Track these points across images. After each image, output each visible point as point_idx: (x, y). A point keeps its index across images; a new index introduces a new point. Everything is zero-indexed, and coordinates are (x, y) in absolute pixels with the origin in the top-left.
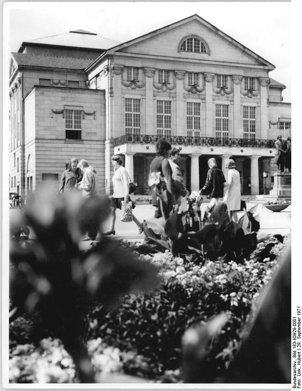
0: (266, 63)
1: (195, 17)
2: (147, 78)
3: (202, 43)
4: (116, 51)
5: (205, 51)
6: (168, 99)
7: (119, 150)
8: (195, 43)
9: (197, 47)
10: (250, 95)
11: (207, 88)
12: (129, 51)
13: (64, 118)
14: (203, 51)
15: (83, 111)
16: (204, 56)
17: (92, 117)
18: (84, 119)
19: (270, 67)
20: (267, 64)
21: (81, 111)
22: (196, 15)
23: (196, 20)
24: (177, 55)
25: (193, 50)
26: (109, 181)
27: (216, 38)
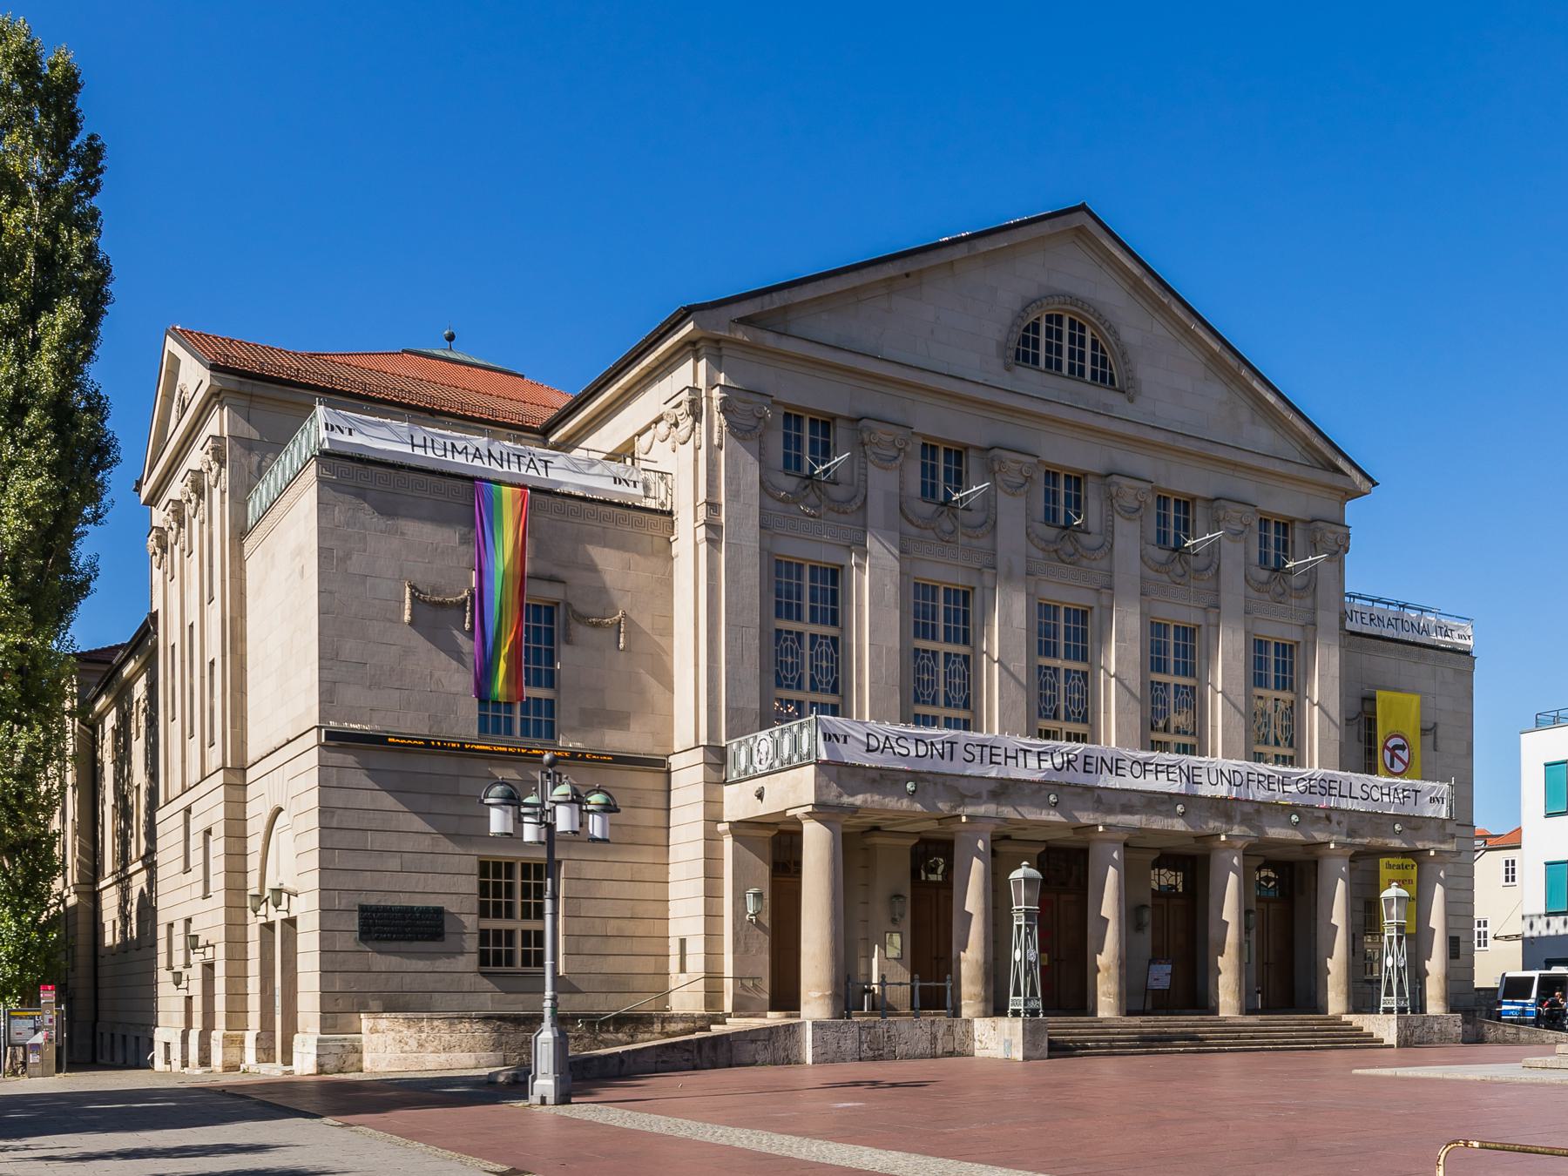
3: (1095, 343)
6: (959, 579)
7: (760, 796)
24: (1006, 380)
25: (1065, 370)
26: (696, 948)
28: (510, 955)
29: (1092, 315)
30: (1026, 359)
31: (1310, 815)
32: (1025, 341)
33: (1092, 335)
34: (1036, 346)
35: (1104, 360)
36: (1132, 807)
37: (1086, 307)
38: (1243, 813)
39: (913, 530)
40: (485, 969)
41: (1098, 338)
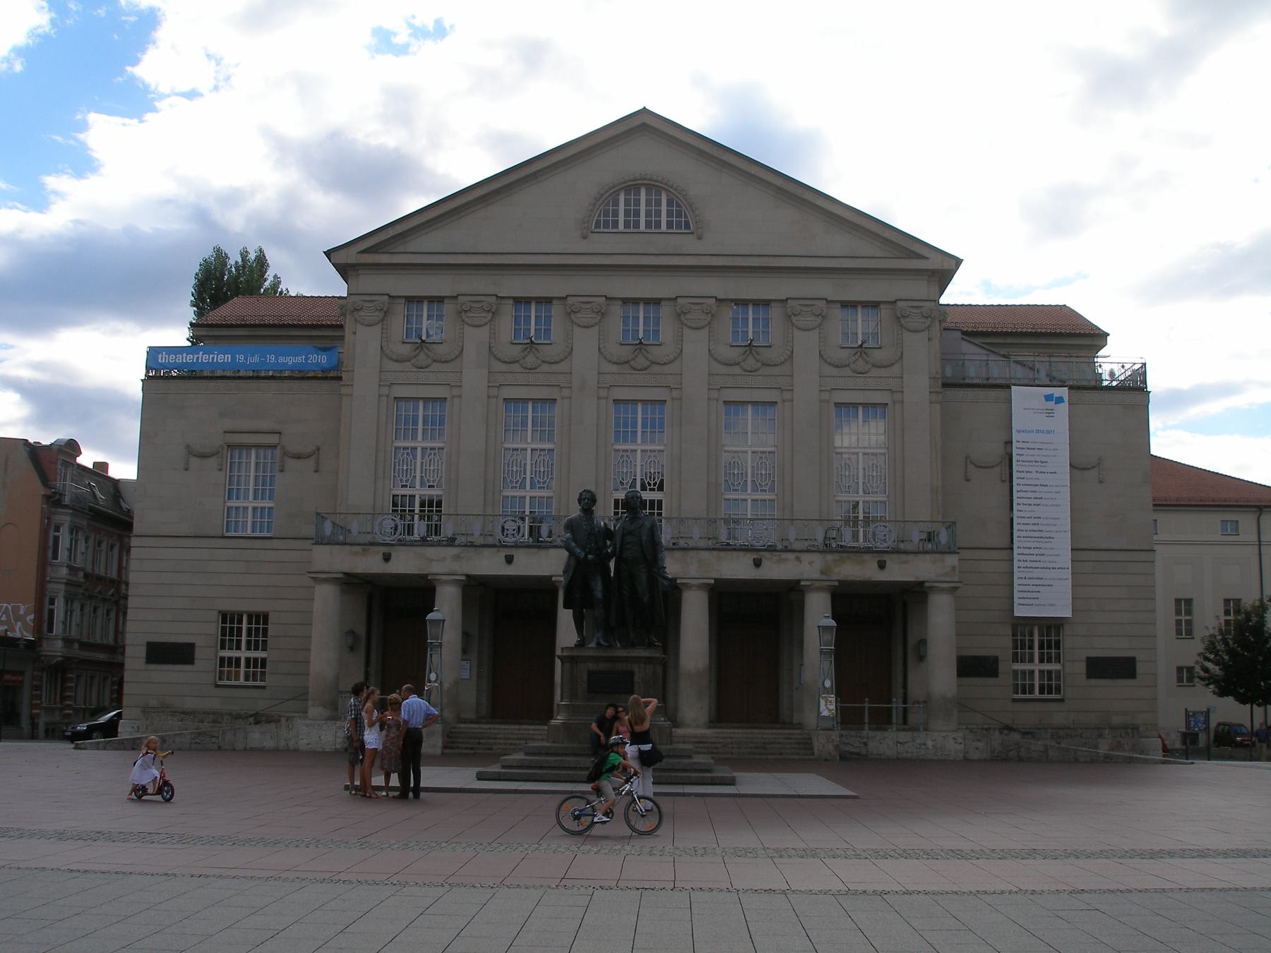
0: (917, 248)
1: (637, 122)
2: (468, 330)
3: (670, 203)
5: (687, 226)
8: (648, 203)
9: (653, 214)
10: (860, 365)
13: (220, 470)
15: (283, 448)
16: (687, 243)
17: (311, 463)
18: (282, 471)
20: (924, 252)
21: (275, 447)
22: (644, 111)
23: (644, 127)
24: (583, 246)
29: (661, 183)
30: (606, 225)
32: (606, 214)
33: (667, 196)
34: (616, 214)
35: (679, 215)
39: (503, 367)
41: (674, 197)
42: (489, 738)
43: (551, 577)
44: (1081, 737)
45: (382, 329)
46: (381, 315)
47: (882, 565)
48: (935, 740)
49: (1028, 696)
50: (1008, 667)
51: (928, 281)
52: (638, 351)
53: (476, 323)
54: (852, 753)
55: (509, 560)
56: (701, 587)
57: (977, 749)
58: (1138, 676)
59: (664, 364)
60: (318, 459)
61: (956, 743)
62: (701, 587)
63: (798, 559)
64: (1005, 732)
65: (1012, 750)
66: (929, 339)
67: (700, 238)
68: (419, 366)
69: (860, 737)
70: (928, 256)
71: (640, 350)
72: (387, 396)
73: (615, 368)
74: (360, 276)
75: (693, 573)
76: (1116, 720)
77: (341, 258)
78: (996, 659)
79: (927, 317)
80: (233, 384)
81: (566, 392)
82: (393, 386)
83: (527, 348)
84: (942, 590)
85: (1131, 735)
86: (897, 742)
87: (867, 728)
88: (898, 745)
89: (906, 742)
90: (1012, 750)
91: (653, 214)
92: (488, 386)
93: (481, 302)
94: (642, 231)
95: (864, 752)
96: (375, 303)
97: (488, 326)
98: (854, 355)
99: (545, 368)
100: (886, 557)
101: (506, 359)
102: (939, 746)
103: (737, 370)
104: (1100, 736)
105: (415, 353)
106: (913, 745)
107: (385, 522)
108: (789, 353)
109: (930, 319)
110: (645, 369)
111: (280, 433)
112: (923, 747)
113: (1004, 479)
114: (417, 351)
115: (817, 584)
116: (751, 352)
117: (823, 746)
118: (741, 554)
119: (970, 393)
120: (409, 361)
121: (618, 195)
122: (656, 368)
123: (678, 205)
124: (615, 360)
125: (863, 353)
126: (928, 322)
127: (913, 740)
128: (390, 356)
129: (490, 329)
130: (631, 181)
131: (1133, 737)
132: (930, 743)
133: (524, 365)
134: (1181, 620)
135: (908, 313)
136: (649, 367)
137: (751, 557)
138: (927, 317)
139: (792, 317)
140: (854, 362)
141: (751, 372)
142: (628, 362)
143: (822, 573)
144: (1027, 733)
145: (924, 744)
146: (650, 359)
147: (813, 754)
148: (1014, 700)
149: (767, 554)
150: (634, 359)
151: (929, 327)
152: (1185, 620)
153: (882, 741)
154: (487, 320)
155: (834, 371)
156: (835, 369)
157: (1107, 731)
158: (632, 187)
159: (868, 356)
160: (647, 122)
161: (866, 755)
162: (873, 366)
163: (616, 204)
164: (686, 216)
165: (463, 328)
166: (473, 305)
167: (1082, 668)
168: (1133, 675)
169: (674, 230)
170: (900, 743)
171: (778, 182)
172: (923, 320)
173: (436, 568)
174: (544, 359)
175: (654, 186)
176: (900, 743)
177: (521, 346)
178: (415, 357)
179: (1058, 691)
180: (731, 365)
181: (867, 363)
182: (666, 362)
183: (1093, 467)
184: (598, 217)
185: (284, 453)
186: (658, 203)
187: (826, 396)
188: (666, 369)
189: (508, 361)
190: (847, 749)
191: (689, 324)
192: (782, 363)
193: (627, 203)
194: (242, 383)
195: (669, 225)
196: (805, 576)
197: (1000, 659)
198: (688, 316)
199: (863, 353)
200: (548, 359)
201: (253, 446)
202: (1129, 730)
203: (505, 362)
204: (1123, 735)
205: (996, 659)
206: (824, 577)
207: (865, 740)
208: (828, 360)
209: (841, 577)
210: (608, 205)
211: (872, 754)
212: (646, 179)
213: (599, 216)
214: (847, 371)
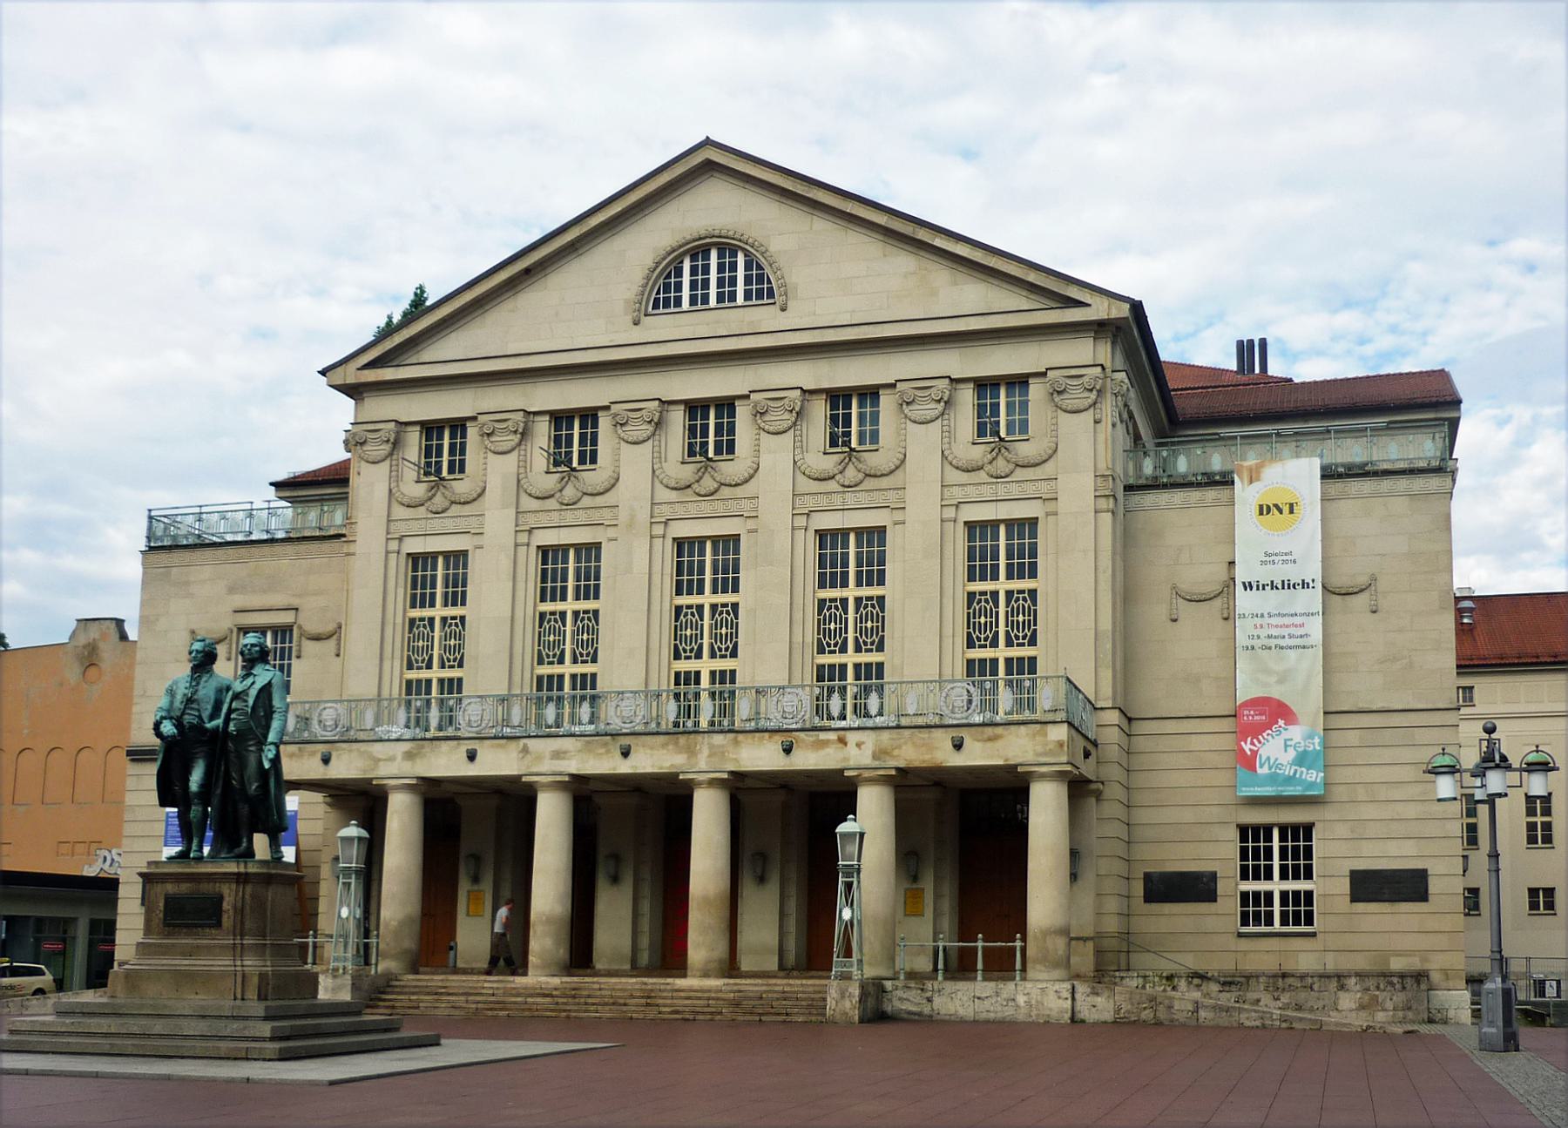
0: (1074, 292)
3: (748, 266)
4: (371, 365)
5: (771, 294)
8: (721, 268)
9: (726, 283)
11: (765, 461)
12: (427, 355)
14: (762, 289)
15: (300, 627)
17: (332, 642)
18: (298, 657)
19: (1099, 310)
23: (709, 167)
24: (636, 335)
27: (822, 226)
28: (1270, 915)
29: (733, 239)
30: (667, 304)
31: (811, 739)
33: (746, 256)
36: (565, 752)
37: (724, 233)
38: (711, 746)
40: (1245, 930)
42: (589, 996)
43: (520, 776)
44: (1311, 988)
45: (391, 466)
46: (387, 447)
47: (958, 746)
48: (1028, 994)
49: (1263, 929)
50: (1232, 886)
51: (1095, 338)
52: (702, 470)
53: (500, 449)
54: (910, 1013)
55: (472, 756)
56: (713, 783)
57: (1094, 1006)
58: (1430, 897)
59: (737, 485)
60: (339, 640)
61: (1059, 998)
62: (713, 783)
63: (842, 741)
64: (1196, 981)
65: (1145, 1008)
66: (1097, 422)
67: (783, 309)
68: (434, 510)
69: (922, 990)
70: (1089, 302)
71: (706, 469)
72: (398, 553)
73: (673, 496)
74: (366, 399)
75: (703, 766)
76: (1397, 964)
77: (339, 377)
78: (1213, 877)
79: (1091, 390)
80: (243, 550)
81: (611, 532)
82: (405, 538)
83: (563, 478)
84: (1043, 776)
85: (1398, 986)
86: (974, 997)
87: (979, 977)
88: (976, 1000)
89: (987, 997)
90: (1145, 1008)
91: (726, 283)
92: (516, 531)
93: (505, 420)
94: (686, 310)
95: (927, 1010)
96: (381, 433)
97: (515, 453)
98: (991, 452)
99: (587, 501)
100: (964, 733)
101: (538, 494)
102: (1033, 1002)
103: (832, 486)
104: (1342, 987)
105: (430, 494)
106: (997, 1001)
107: (325, 713)
108: (902, 456)
109: (1095, 392)
110: (712, 494)
111: (297, 609)
112: (1010, 1004)
113: (1225, 615)
114: (433, 491)
115: (866, 774)
116: (850, 459)
117: (837, 1002)
118: (766, 735)
119: (1178, 496)
120: (422, 505)
121: (682, 262)
122: (726, 492)
123: (759, 267)
124: (673, 484)
125: (1003, 450)
126: (1093, 395)
127: (997, 994)
128: (399, 499)
129: (519, 455)
130: (694, 240)
131: (1404, 988)
132: (1021, 1000)
133: (560, 500)
134: (1542, 815)
135: (1063, 387)
136: (716, 491)
137: (778, 738)
138: (1091, 390)
139: (904, 406)
140: (990, 463)
141: (849, 487)
142: (689, 486)
143: (875, 757)
144: (1230, 983)
145: (1014, 1000)
146: (718, 479)
147: (825, 1015)
148: (1240, 935)
149: (802, 735)
150: (698, 481)
151: (1095, 403)
152: (1536, 815)
153: (953, 995)
154: (513, 443)
155: (964, 478)
156: (965, 474)
157: (1353, 980)
158: (698, 251)
159: (1010, 453)
160: (711, 158)
161: (931, 1016)
162: (1017, 465)
163: (679, 273)
164: (769, 282)
165: (485, 458)
166: (498, 425)
167: (1345, 886)
168: (1422, 895)
169: (754, 302)
170: (979, 998)
171: (881, 219)
172: (1086, 394)
173: (384, 770)
174: (585, 491)
175: (727, 248)
176: (979, 998)
177: (558, 475)
178: (430, 499)
179: (1309, 922)
180: (825, 479)
181: (1008, 461)
182: (739, 481)
183: (1362, 591)
184: (657, 294)
185: (301, 634)
186: (733, 267)
187: (950, 513)
188: (739, 491)
189: (540, 495)
190: (903, 1007)
191: (767, 427)
192: (892, 472)
193: (694, 271)
194: (254, 550)
195: (748, 295)
196: (852, 763)
197: (1218, 875)
198: (767, 418)
199: (1003, 450)
200: (590, 491)
201: (270, 628)
202: (1395, 980)
203: (537, 498)
204: (1382, 986)
205: (1213, 877)
206: (876, 764)
207: (929, 994)
208: (954, 462)
209: (902, 764)
210: (669, 276)
211: (938, 1014)
212: (713, 236)
213: (658, 293)
214: (982, 476)
